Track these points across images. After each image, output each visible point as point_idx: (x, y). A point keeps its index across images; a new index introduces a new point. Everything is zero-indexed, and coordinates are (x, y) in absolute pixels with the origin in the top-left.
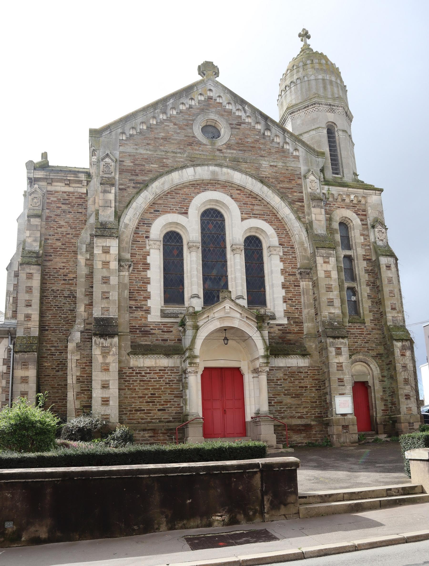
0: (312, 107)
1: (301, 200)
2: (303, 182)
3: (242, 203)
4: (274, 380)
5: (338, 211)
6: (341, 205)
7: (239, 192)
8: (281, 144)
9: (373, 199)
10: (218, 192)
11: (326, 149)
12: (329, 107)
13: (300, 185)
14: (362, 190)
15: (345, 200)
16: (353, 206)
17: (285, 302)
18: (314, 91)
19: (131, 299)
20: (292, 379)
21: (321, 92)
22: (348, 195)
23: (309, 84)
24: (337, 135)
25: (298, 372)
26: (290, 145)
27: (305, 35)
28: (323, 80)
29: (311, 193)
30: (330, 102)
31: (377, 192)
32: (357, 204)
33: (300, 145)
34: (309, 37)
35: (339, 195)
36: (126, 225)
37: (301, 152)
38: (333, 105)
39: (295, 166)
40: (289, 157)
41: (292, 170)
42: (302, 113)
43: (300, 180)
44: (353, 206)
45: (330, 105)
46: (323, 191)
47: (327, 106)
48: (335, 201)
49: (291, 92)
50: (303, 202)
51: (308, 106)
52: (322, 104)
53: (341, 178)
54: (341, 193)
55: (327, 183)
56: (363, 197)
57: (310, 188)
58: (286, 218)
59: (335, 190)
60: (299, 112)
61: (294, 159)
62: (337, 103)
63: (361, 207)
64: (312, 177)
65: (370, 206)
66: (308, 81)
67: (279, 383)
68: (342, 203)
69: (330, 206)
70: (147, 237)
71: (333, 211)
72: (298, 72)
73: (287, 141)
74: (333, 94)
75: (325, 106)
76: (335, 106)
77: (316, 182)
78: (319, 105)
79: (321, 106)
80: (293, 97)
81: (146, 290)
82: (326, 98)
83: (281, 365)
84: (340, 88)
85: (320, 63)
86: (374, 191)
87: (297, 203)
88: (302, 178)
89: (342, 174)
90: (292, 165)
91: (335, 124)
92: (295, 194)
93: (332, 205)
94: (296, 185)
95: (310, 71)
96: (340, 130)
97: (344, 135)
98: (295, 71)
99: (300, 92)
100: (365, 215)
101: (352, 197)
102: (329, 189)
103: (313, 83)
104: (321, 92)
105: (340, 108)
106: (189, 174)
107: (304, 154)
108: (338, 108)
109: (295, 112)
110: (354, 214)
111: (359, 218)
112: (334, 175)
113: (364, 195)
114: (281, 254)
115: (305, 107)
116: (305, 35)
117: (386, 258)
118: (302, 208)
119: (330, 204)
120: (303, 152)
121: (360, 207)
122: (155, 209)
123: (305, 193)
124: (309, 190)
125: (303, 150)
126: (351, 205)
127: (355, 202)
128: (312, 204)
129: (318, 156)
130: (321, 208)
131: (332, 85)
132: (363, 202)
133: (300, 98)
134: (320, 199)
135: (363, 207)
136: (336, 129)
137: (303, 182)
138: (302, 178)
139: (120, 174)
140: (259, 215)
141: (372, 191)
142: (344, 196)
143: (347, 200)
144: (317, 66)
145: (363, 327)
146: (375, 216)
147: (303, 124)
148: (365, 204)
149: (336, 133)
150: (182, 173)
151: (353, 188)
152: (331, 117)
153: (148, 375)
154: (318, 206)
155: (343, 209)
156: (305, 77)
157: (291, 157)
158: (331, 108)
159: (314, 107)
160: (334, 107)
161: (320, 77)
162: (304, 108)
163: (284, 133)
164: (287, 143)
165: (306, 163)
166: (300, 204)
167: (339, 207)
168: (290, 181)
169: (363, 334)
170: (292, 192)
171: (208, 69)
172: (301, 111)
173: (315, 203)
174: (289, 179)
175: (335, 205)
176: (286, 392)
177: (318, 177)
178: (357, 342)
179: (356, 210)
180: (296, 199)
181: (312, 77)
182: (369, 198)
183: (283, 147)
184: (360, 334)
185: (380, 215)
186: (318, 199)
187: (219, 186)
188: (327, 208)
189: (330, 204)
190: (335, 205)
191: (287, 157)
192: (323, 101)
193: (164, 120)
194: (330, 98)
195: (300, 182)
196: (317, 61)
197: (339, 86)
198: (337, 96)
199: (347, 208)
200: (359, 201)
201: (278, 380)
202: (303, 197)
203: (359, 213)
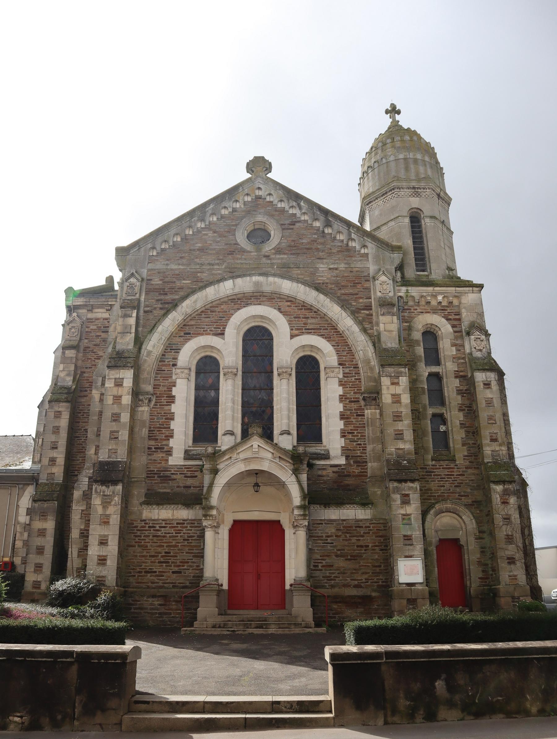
0: (391, 193)
1: (369, 307)
2: (372, 285)
3: (292, 317)
4: (322, 537)
5: (420, 317)
6: (425, 309)
7: (289, 303)
8: (345, 242)
9: (469, 298)
10: (263, 306)
11: (408, 242)
12: (413, 190)
13: (368, 289)
14: (453, 289)
15: (430, 302)
16: (442, 310)
17: (343, 436)
18: (393, 173)
19: (150, 438)
20: (348, 535)
21: (402, 174)
22: (435, 296)
23: (387, 167)
24: (423, 223)
25: (356, 527)
26: (357, 241)
27: (393, 111)
28: (405, 159)
29: (380, 298)
30: (414, 184)
31: (475, 289)
32: (447, 307)
33: (369, 240)
34: (399, 112)
35: (422, 296)
36: (149, 353)
37: (371, 249)
38: (418, 188)
39: (362, 266)
40: (355, 257)
41: (357, 271)
42: (380, 202)
43: (367, 283)
44: (442, 310)
45: (414, 188)
46: (400, 294)
47: (410, 190)
48: (416, 305)
49: (368, 179)
50: (371, 309)
51: (386, 193)
52: (403, 188)
53: (427, 276)
54: (425, 294)
55: (405, 282)
56: (455, 296)
57: (380, 292)
58: (347, 331)
59: (415, 291)
60: (376, 201)
61: (361, 259)
62: (423, 184)
63: (454, 310)
64: (383, 278)
65: (465, 308)
66: (387, 162)
67: (329, 541)
68: (426, 307)
69: (409, 312)
70: (174, 365)
71: (414, 318)
72: (376, 154)
73: (353, 237)
74: (417, 174)
76: (420, 189)
77: (388, 284)
78: (399, 190)
79: (402, 190)
80: (370, 184)
81: (169, 428)
82: (408, 180)
83: (333, 517)
84: (428, 166)
85: (402, 141)
86: (471, 289)
87: (362, 311)
88: (371, 279)
89: (429, 270)
90: (358, 265)
91: (421, 210)
92: (361, 300)
93: (412, 311)
94: (362, 290)
95: (389, 151)
96: (426, 217)
97: (433, 222)
98: (373, 154)
99: (377, 177)
100: (459, 320)
101: (440, 298)
102: (407, 290)
103: (393, 165)
104: (402, 174)
105: (428, 190)
106: (227, 287)
107: (374, 251)
108: (425, 190)
109: (372, 202)
110: (444, 320)
111: (449, 324)
112: (418, 273)
113: (456, 294)
114: (341, 376)
115: (384, 194)
116: (393, 111)
117: (484, 374)
118: (370, 317)
119: (410, 309)
120: (372, 249)
121: (451, 310)
122: (186, 331)
123: (375, 298)
124: (379, 294)
125: (374, 246)
126: (440, 308)
127: (445, 303)
128: (381, 311)
129: (392, 251)
130: (393, 315)
131: (417, 164)
132: (456, 302)
133: (377, 184)
134: (391, 304)
135: (456, 310)
136: (422, 216)
137: (372, 285)
138: (371, 279)
139: (146, 294)
140: (314, 329)
141: (467, 289)
142: (429, 298)
143: (434, 303)
144: (398, 144)
145: (452, 466)
146: (471, 319)
147: (381, 215)
148: (459, 306)
149: (423, 221)
150: (218, 287)
151: (440, 287)
152: (415, 202)
153: (163, 529)
154: (389, 313)
155: (428, 314)
156: (384, 159)
157: (358, 256)
158: (416, 192)
159: (393, 193)
160: (419, 190)
161: (401, 156)
162: (382, 196)
163: (349, 228)
164: (353, 240)
165: (376, 261)
166: (367, 312)
167: (423, 312)
168: (355, 284)
169: (453, 475)
170: (356, 298)
171: (259, 166)
172: (379, 200)
173: (384, 310)
174: (354, 283)
175: (416, 309)
176: (339, 552)
177: (391, 278)
178: (444, 486)
179: (446, 313)
180: (361, 306)
181: (392, 158)
182: (463, 297)
183: (347, 245)
184: (448, 475)
185: (479, 317)
186: (388, 305)
187: (264, 299)
188: (406, 314)
189: (410, 309)
190: (416, 309)
191: (352, 257)
192: (404, 184)
193: (202, 228)
194: (414, 180)
195: (368, 285)
196: (399, 138)
197: (427, 163)
198: (423, 176)
199: (433, 313)
200: (450, 303)
201: (328, 536)
202: (371, 303)
203: (450, 317)
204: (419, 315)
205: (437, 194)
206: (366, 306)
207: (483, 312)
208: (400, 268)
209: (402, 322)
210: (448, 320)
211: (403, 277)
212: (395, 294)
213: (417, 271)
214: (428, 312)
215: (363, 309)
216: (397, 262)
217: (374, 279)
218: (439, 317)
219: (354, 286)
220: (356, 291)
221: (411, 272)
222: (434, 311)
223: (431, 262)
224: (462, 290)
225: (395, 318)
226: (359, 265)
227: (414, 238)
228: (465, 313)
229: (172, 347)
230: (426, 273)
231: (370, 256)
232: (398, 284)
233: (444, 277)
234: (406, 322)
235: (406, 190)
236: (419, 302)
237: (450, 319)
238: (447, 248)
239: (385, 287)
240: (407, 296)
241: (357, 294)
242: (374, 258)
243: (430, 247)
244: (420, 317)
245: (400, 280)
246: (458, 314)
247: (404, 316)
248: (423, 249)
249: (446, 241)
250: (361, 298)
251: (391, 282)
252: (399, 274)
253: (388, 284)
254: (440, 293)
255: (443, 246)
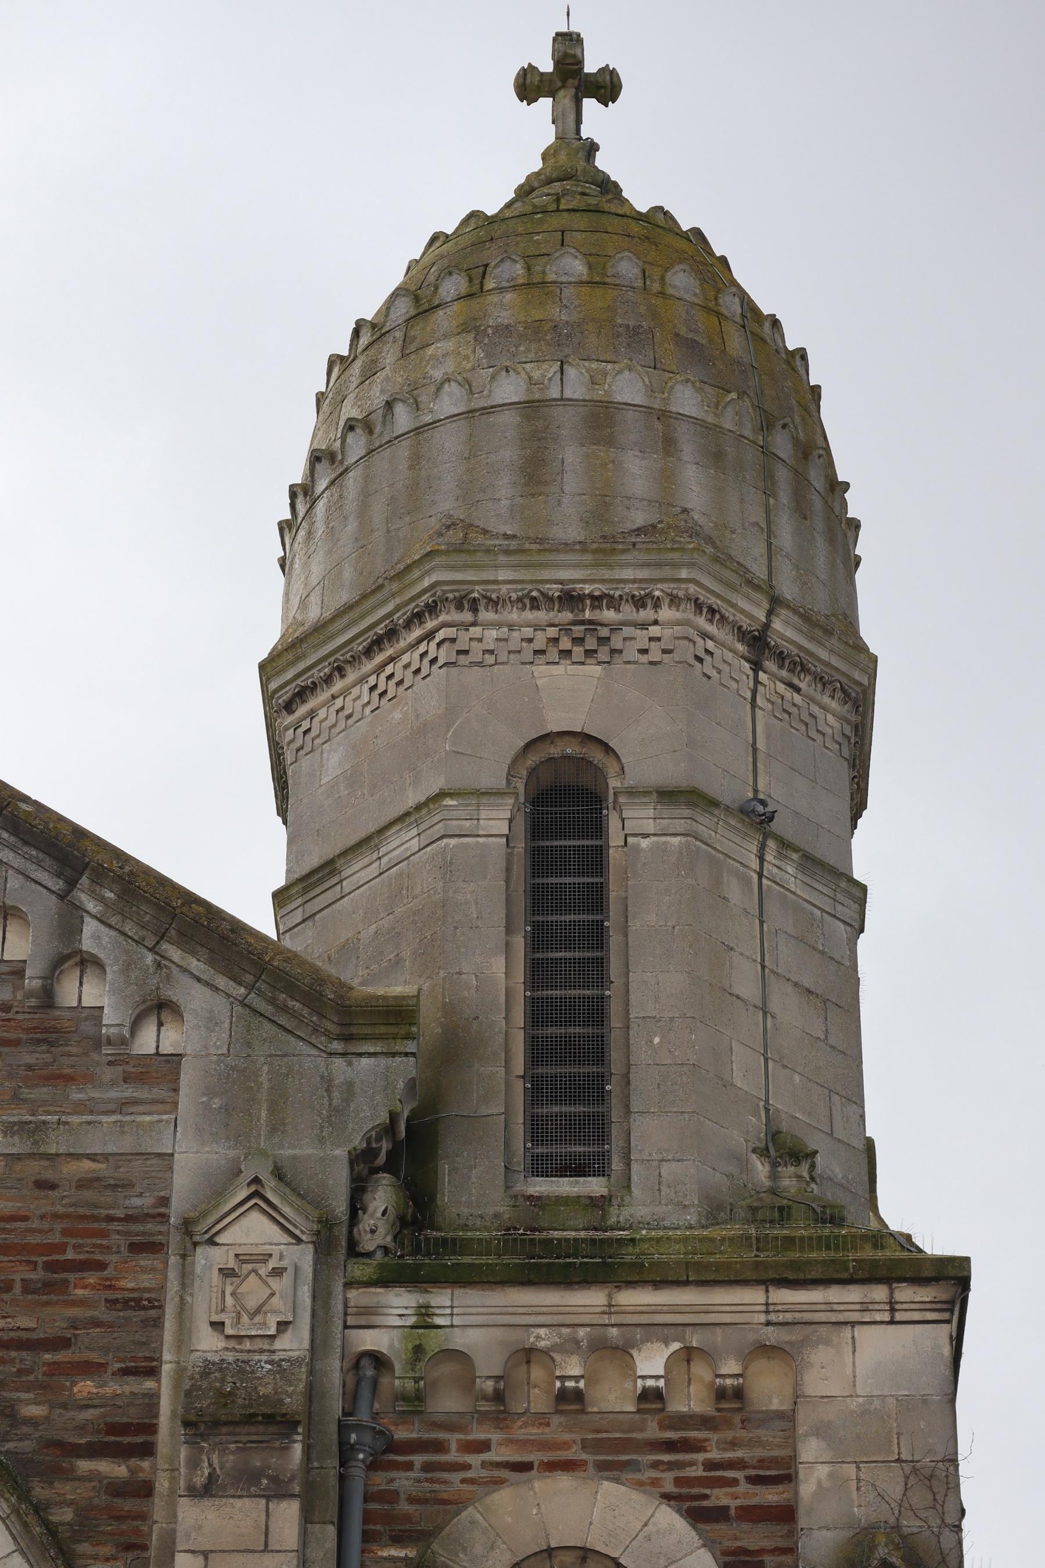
0: (417, 633)
1: (132, 1437)
2: (173, 1275)
5: (502, 1499)
6: (545, 1445)
8: (32, 981)
9: (868, 1355)
11: (491, 973)
12: (567, 616)
13: (146, 1308)
14: (754, 1296)
15: (578, 1396)
16: (670, 1446)
18: (445, 503)
21: (499, 510)
22: (613, 1350)
23: (416, 460)
24: (615, 838)
26: (112, 971)
27: (569, 79)
28: (532, 408)
29: (207, 1369)
30: (570, 573)
31: (905, 1293)
32: (705, 1422)
33: (195, 965)
34: (607, 88)
35: (528, 1354)
37: (200, 1026)
38: (597, 601)
39: (125, 1144)
40: (89, 1079)
41: (84, 1183)
42: (354, 691)
43: (145, 1261)
44: (670, 1446)
45: (570, 599)
46: (370, 1340)
47: (541, 616)
48: (483, 1417)
50: (147, 1450)
51: (392, 634)
52: (494, 603)
53: (599, 1204)
54: (544, 1338)
55: (425, 1253)
56: (766, 1350)
57: (218, 1326)
59: (477, 1321)
60: (338, 685)
61: (129, 1092)
62: (629, 573)
63: (751, 1444)
64: (254, 1231)
65: (821, 1431)
66: (418, 430)
68: (557, 1430)
69: (427, 1467)
71: (459, 1504)
72: (369, 374)
73: (87, 944)
74: (603, 503)
75: (529, 615)
76: (614, 603)
77: (277, 1272)
78: (467, 616)
79: (486, 615)
80: (317, 570)
82: (543, 547)
84: (688, 448)
85: (535, 287)
86: (879, 1293)
87: (84, 1465)
88: (175, 1240)
89: (617, 1165)
90: (94, 1135)
91: (607, 749)
92: (85, 1387)
93: (453, 1456)
94: (101, 1313)
96: (632, 792)
97: (680, 825)
98: (357, 368)
99: (352, 526)
100: (786, 1515)
101: (652, 1363)
102: (424, 1312)
104: (499, 510)
105: (666, 613)
107: (219, 1041)
108: (646, 614)
109: (313, 688)
110: (669, 1520)
111: (708, 1544)
112: (541, 1186)
113: (773, 1336)
115: (378, 643)
116: (569, 79)
118: (129, 1505)
119: (439, 1447)
120: (211, 1022)
121: (733, 1444)
123: (180, 1371)
124: (208, 1344)
125: (221, 1006)
126: (653, 1431)
127: (692, 1400)
128: (194, 1464)
129: (347, 1038)
130: (278, 1491)
131: (610, 442)
132: (769, 1389)
133: (348, 573)
134: (270, 1419)
135: (769, 1443)
136: (613, 783)
137: (173, 1275)
138: (175, 1240)
141: (853, 1294)
142: (573, 1367)
143: (614, 1398)
144: (503, 309)
146: (864, 1510)
147: (352, 778)
148: (788, 1418)
149: (613, 823)
151: (658, 1284)
152: (569, 695)
154: (248, 1481)
155: (564, 1481)
156: (400, 409)
157: (108, 1074)
158: (581, 623)
159: (429, 636)
160: (609, 615)
161: (509, 390)
162: (368, 652)
163: (72, 884)
164: (87, 962)
165: (227, 1110)
166: (116, 1470)
167: (524, 1467)
168: (57, 1274)
170: (55, 1369)
172: (351, 676)
173: (218, 1459)
174: (52, 1267)
175: (484, 1446)
177: (304, 1226)
179: (698, 1472)
180: (82, 1428)
181: (450, 402)
182: (819, 1356)
183: (47, 997)
185: (919, 1497)
186: (249, 1419)
188: (404, 1482)
189: (439, 1447)
190: (484, 1446)
191: (70, 1079)
192: (505, 575)
194: (567, 547)
195: (146, 1281)
196: (518, 269)
197: (685, 434)
198: (639, 518)
199: (603, 1467)
200: (721, 1394)
202: (152, 1400)
203: (720, 1497)
204: (499, 1482)
205: (742, 634)
206: (113, 1429)
207: (954, 1461)
208: (409, 1150)
209: (368, 1537)
210: (699, 1516)
211: (418, 1211)
212: (317, 1346)
213: (540, 1167)
214: (569, 1466)
215: (94, 1451)
216: (368, 1115)
217: (196, 1234)
218: (636, 1496)
219: (48, 1286)
220: (55, 1319)
221: (478, 1187)
222: (611, 1456)
223: (636, 1105)
224: (812, 1307)
225: (287, 1515)
226: (104, 1136)
227: (540, 938)
228: (823, 1471)
230: (594, 1186)
231: (188, 1076)
232: (359, 1270)
233: (716, 1210)
234: (397, 1540)
235: (514, 615)
236: (499, 1397)
237: (720, 1514)
238: (786, 1005)
239: (253, 1290)
240: (418, 1350)
241: (61, 1343)
242: (210, 1092)
243: (642, 1004)
244: (503, 1500)
245: (383, 1237)
246: (783, 1472)
247: (391, 1497)
248: (596, 1012)
249: (787, 956)
250: (88, 1369)
251: (305, 1257)
252: (383, 1198)
253: (277, 1272)
254: (655, 1331)
255: (747, 986)
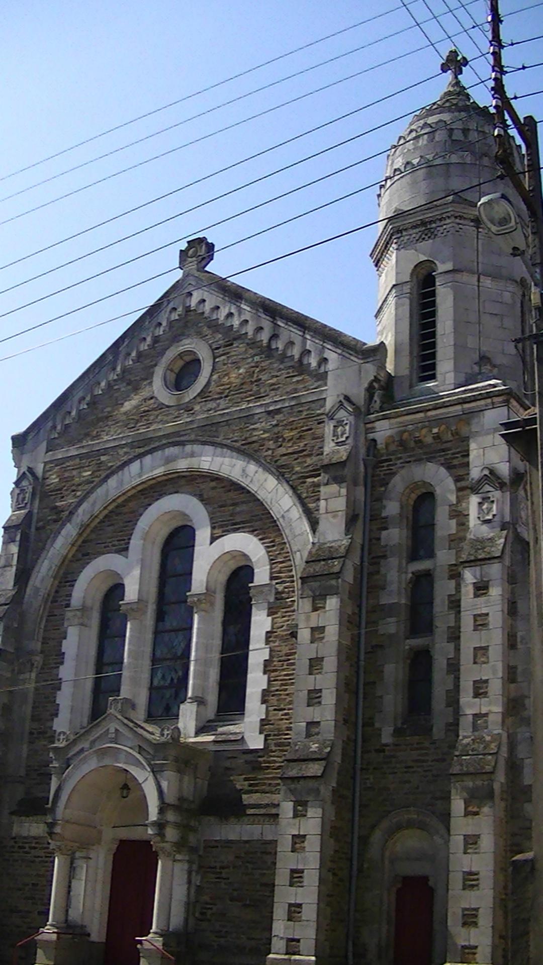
3: (216, 506)
4: (215, 867)
7: (213, 484)
10: (183, 495)
17: (264, 702)
19: (34, 718)
20: (250, 866)
25: (262, 853)
31: (496, 399)
33: (329, 347)
45: (423, 223)
47: (417, 230)
52: (406, 230)
58: (281, 520)
67: (224, 875)
69: (388, 466)
70: (68, 605)
73: (308, 347)
75: (415, 231)
79: (404, 233)
81: (55, 701)
83: (232, 837)
86: (489, 401)
105: (448, 221)
106: (136, 474)
111: (451, 475)
114: (272, 600)
117: (478, 568)
122: (84, 552)
140: (243, 522)
141: (482, 402)
145: (427, 744)
150: (123, 474)
153: (33, 851)
160: (434, 225)
169: (426, 761)
176: (235, 893)
178: (409, 782)
184: (417, 761)
187: (183, 482)
189: (390, 460)
190: (400, 458)
193: (115, 380)
201: (222, 868)
203: (455, 462)
205: (472, 221)
229: (66, 577)
235: (411, 232)
237: (454, 467)
